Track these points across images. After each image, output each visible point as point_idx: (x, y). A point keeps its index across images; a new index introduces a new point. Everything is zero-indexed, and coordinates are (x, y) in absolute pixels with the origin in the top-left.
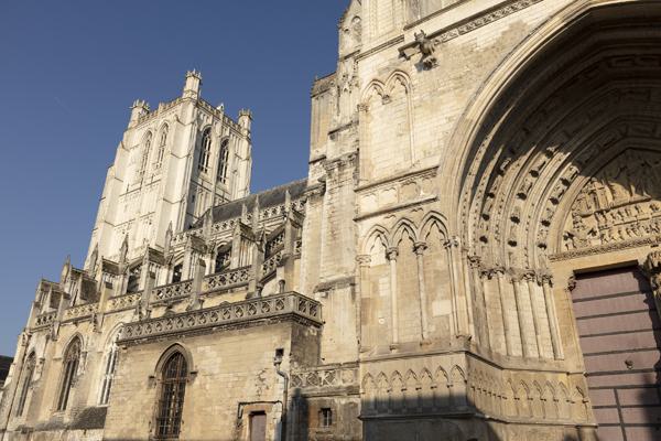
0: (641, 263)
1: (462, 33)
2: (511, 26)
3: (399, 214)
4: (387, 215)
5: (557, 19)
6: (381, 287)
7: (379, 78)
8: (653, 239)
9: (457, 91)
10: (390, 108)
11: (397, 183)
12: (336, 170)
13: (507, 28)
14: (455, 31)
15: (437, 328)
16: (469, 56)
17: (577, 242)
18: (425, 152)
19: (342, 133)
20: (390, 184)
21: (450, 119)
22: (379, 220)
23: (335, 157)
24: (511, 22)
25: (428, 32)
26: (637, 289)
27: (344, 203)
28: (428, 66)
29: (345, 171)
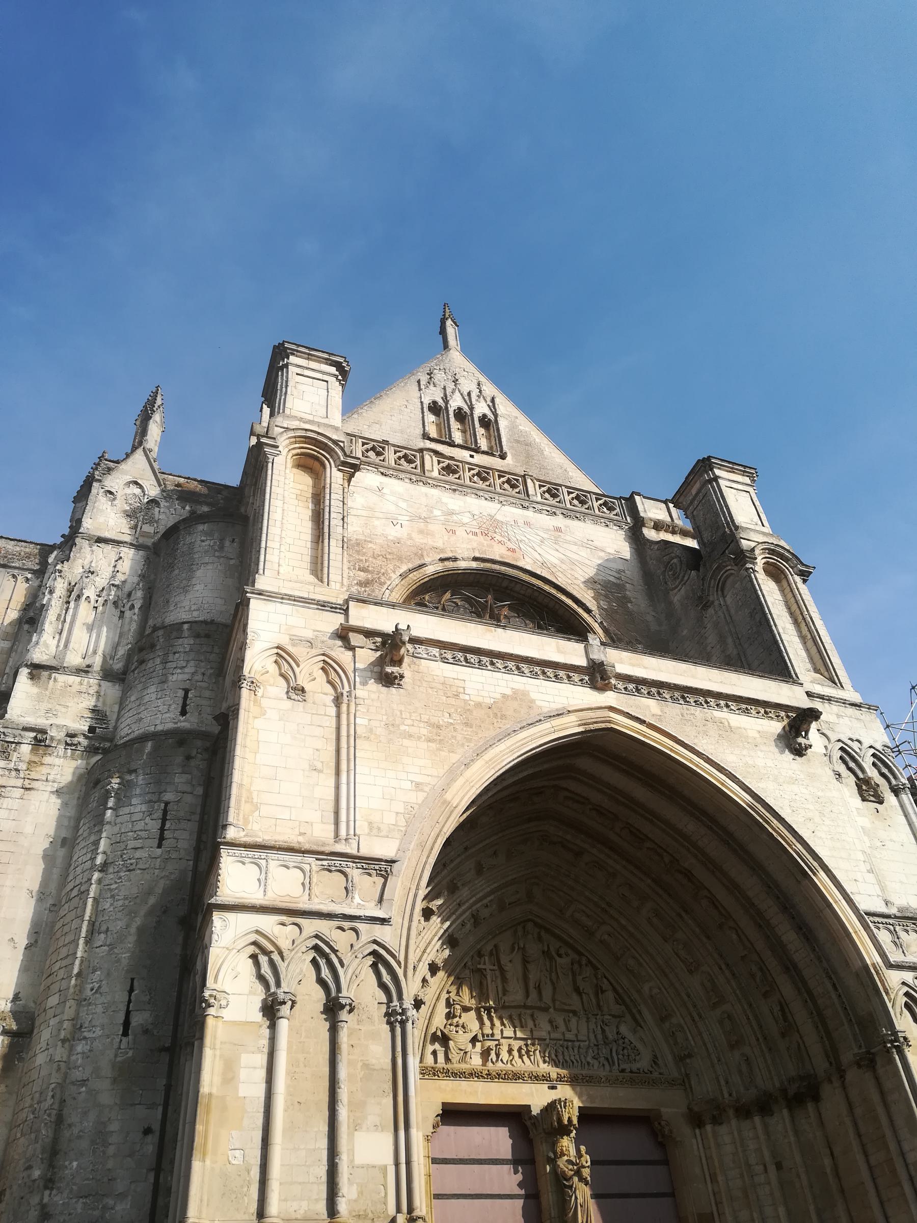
0: (535, 1111)
1: (444, 660)
2: (515, 692)
3: (311, 926)
4: (284, 918)
5: (573, 718)
6: (243, 1074)
7: (290, 649)
8: (554, 1076)
9: (433, 745)
10: (298, 712)
11: (311, 859)
12: (26, 749)
13: (508, 692)
14: (435, 651)
15: (361, 1193)
16: (452, 701)
17: (455, 1056)
18: (370, 823)
19: (62, 678)
20: (298, 858)
21: (418, 786)
22: (268, 923)
23: (31, 721)
24: (516, 686)
25: (416, 632)
26: (509, 1157)
27: (29, 829)
28: (389, 681)
29: (47, 760)
